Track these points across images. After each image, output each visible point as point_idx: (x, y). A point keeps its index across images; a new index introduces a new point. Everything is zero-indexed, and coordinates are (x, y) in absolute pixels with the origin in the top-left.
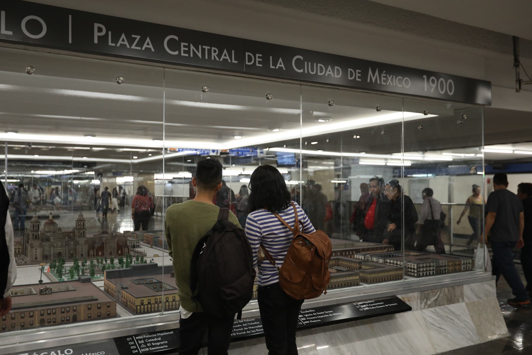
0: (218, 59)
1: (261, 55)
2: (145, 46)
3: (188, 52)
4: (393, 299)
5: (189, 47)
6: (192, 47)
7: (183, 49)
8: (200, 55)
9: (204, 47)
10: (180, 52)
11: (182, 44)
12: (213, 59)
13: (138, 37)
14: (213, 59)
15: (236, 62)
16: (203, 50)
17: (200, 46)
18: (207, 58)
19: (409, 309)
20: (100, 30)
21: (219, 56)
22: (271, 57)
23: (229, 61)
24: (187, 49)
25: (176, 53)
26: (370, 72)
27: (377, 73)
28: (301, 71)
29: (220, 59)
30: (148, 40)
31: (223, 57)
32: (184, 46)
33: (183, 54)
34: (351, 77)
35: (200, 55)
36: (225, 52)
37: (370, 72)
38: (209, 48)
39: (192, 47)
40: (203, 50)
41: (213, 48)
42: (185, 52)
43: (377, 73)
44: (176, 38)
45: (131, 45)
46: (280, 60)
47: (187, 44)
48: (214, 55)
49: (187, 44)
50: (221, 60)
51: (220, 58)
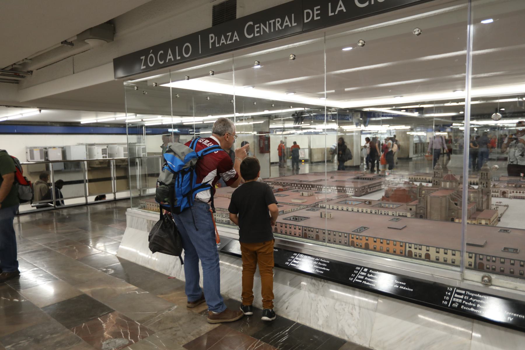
0: (280, 28)
1: (319, 7)
2: (234, 38)
5: (259, 27)
6: (262, 26)
7: (256, 30)
8: (267, 30)
9: (270, 22)
10: (254, 35)
11: (256, 26)
12: (277, 29)
13: (230, 34)
14: (277, 29)
15: (296, 24)
16: (270, 24)
17: (267, 22)
18: (272, 31)
22: (330, 4)
23: (290, 26)
24: (258, 29)
25: (252, 36)
28: (367, 4)
29: (282, 27)
30: (236, 33)
31: (285, 24)
32: (257, 28)
33: (256, 35)
34: (307, 19)
35: (267, 30)
36: (287, 18)
38: (274, 20)
40: (270, 24)
41: (277, 20)
42: (258, 32)
44: (251, 23)
45: (226, 42)
46: (341, 3)
47: (258, 25)
48: (278, 25)
49: (258, 25)
50: (283, 28)
51: (282, 27)
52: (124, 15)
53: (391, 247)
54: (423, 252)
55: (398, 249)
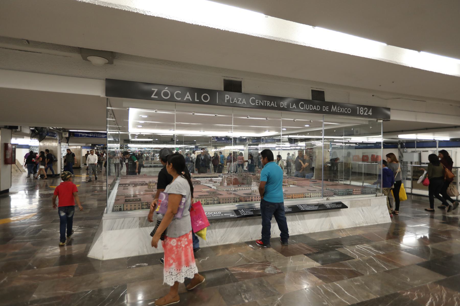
3: (258, 103)
4: (340, 203)
5: (259, 101)
6: (260, 101)
16: (264, 102)
19: (347, 207)
20: (227, 97)
21: (270, 104)
26: (333, 107)
27: (336, 107)
37: (333, 107)
39: (260, 101)
40: (264, 102)
43: (336, 107)
48: (268, 104)
52: (135, 56)
53: (300, 196)
54: (309, 195)
55: (302, 196)
